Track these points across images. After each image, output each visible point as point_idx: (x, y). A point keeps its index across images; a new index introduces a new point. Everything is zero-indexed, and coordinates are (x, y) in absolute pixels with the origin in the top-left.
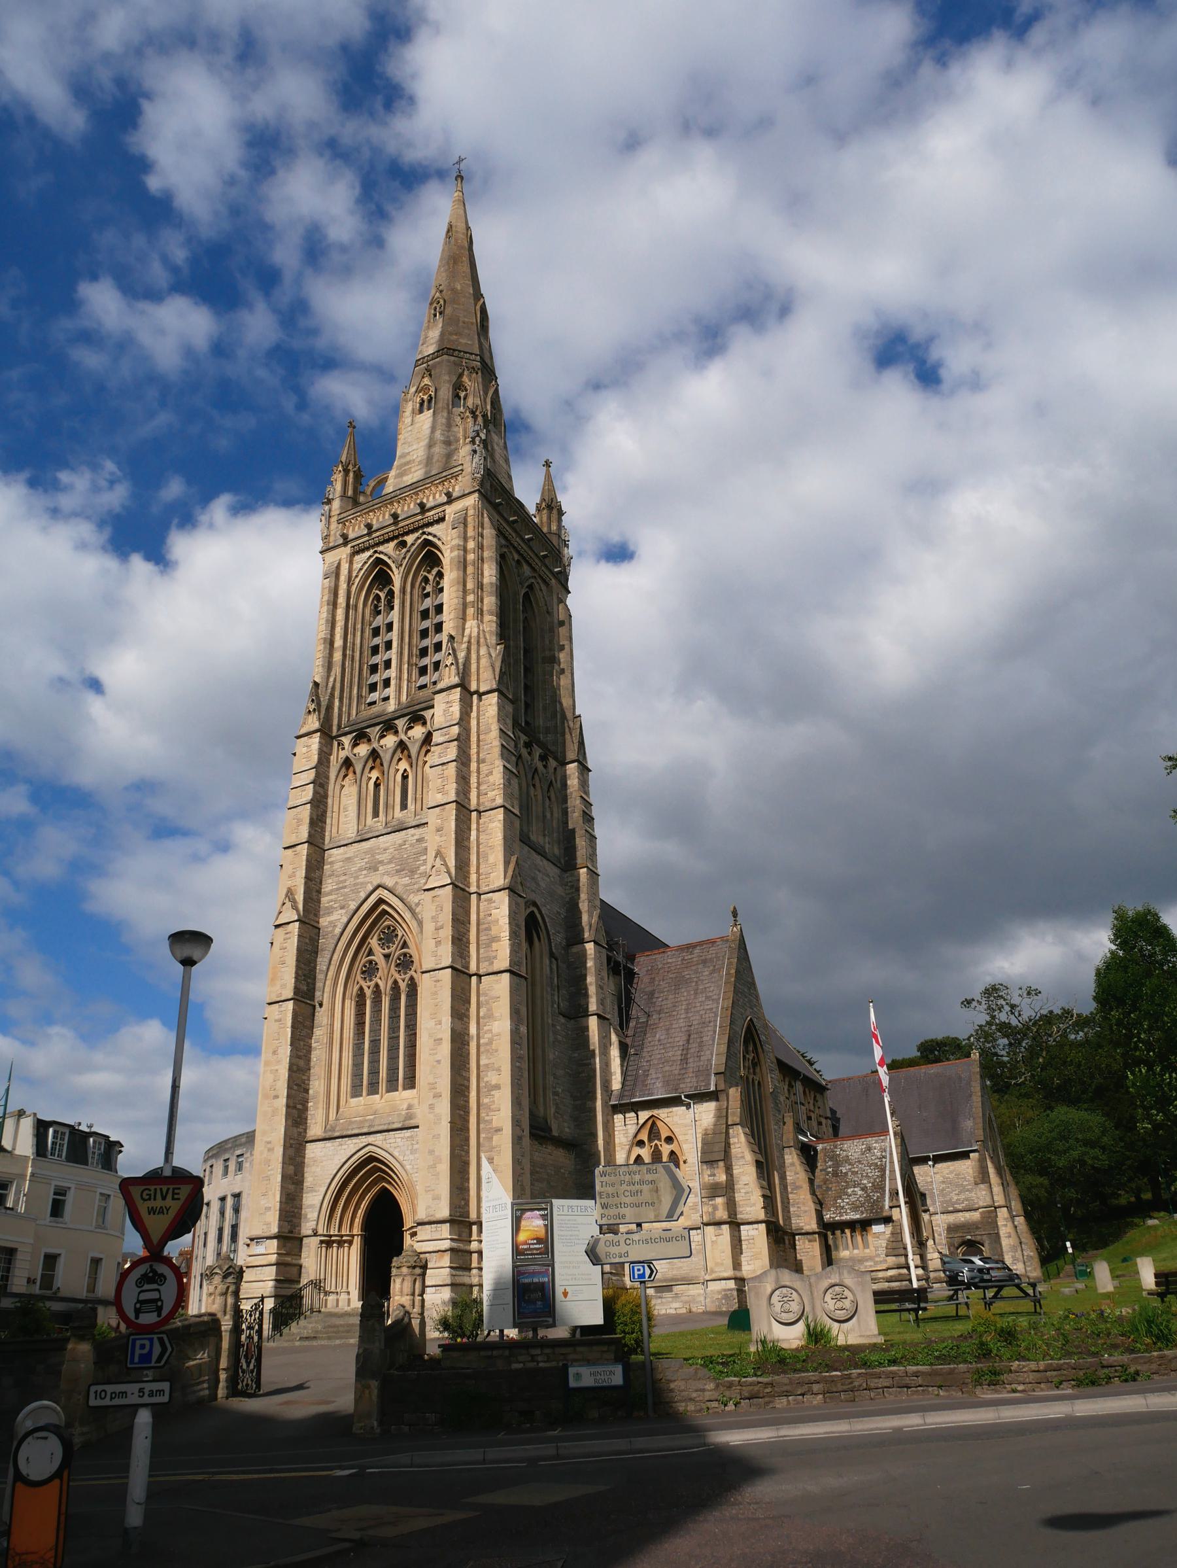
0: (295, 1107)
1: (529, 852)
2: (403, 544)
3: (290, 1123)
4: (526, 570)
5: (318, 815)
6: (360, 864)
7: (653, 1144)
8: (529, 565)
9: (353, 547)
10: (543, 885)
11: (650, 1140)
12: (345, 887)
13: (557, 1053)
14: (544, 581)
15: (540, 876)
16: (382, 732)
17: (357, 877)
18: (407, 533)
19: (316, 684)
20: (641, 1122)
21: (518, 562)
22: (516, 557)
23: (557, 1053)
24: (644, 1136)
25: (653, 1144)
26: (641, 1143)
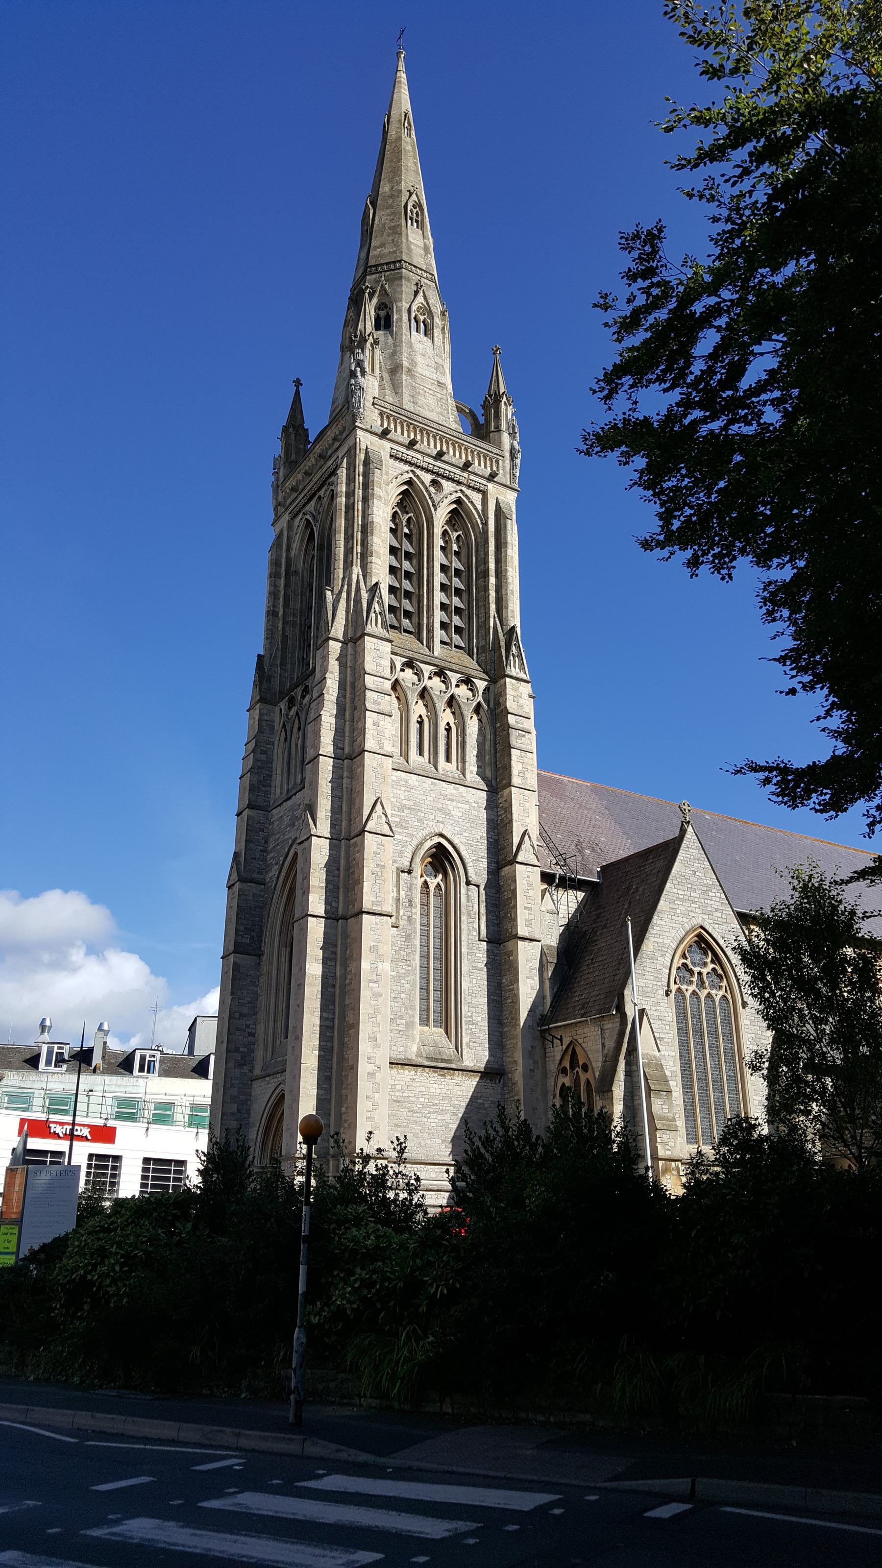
0: (237, 1050)
1: (432, 784)
2: (320, 497)
3: (231, 1064)
4: (448, 486)
5: (259, 781)
6: (286, 820)
7: (575, 1071)
8: (448, 479)
9: (290, 513)
10: (456, 813)
11: (572, 1067)
12: (278, 844)
13: (475, 981)
14: (478, 490)
15: (451, 806)
16: (302, 693)
17: (284, 835)
18: (319, 489)
19: (259, 655)
20: (564, 1047)
21: (434, 483)
22: (427, 478)
23: (475, 981)
24: (567, 1064)
25: (575, 1071)
26: (564, 1071)
